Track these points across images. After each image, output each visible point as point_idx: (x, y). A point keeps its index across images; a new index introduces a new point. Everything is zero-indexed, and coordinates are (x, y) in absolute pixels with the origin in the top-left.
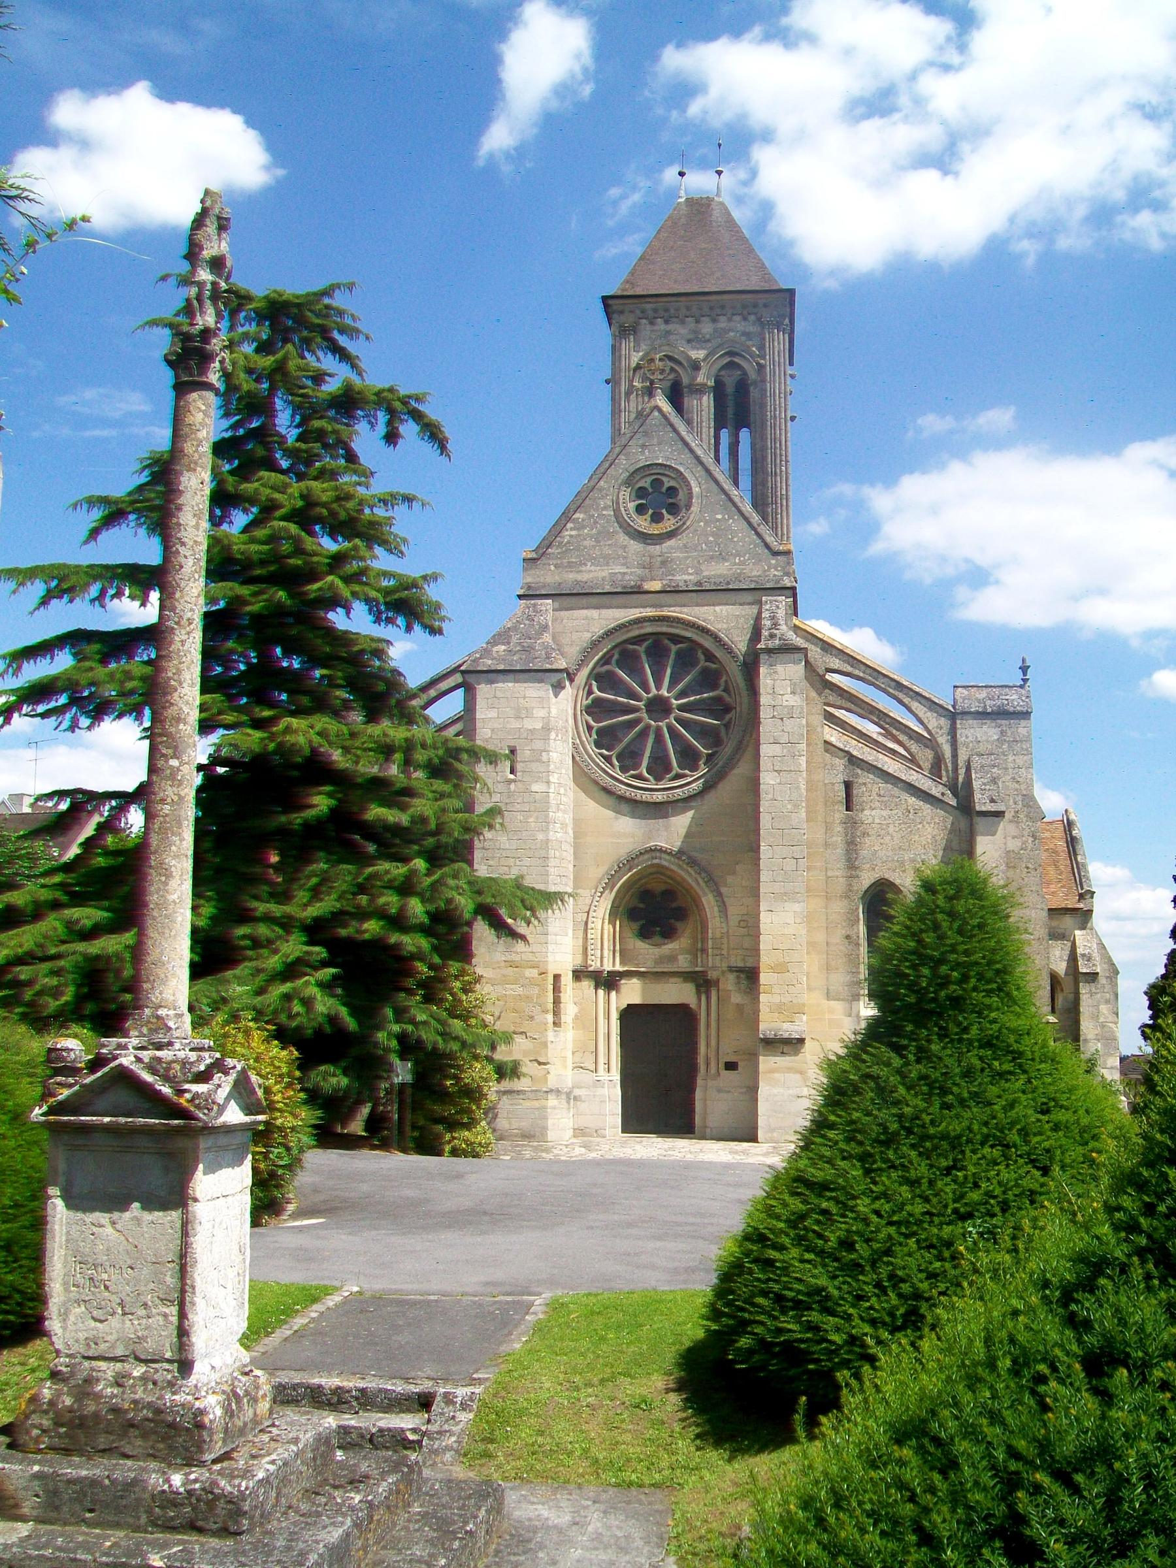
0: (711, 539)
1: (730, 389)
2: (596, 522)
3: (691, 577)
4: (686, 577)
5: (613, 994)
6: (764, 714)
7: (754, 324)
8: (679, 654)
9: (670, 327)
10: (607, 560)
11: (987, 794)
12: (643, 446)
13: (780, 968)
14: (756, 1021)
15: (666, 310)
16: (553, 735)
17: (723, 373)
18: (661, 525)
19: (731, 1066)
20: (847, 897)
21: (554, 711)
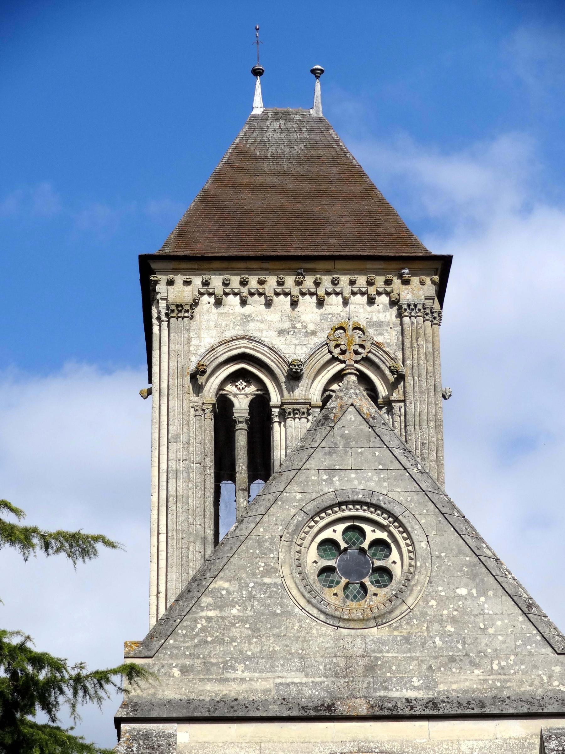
0: (450, 628)
2: (251, 597)
3: (420, 694)
4: (411, 694)
12: (331, 470)
15: (244, 283)
18: (364, 604)
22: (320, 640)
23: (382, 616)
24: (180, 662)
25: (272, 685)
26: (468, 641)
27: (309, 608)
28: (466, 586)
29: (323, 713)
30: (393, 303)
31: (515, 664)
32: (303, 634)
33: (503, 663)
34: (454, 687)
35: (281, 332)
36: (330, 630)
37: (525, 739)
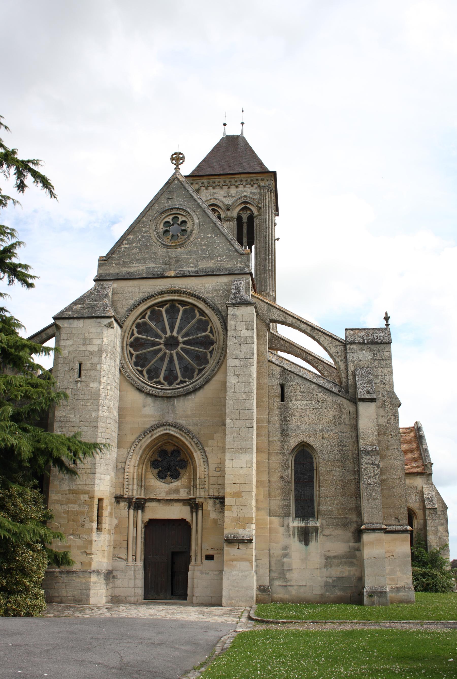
0: (204, 247)
1: (245, 220)
2: (140, 240)
3: (193, 269)
4: (190, 269)
5: (140, 512)
6: (230, 342)
7: (256, 188)
8: (185, 312)
9: (215, 191)
10: (145, 260)
11: (365, 389)
12: (168, 199)
13: (238, 495)
14: (223, 529)
15: (214, 182)
16: (104, 355)
17: (241, 212)
19: (210, 558)
20: (282, 453)
21: (106, 341)
22: (161, 253)
23: (182, 244)
24: (116, 262)
25: (145, 268)
26: (210, 251)
27: (158, 243)
28: (210, 234)
29: (160, 276)
30: (259, 186)
31: (225, 258)
32: (155, 251)
33: (222, 258)
34: (204, 266)
35: (224, 197)
36: (165, 250)
37: (227, 282)
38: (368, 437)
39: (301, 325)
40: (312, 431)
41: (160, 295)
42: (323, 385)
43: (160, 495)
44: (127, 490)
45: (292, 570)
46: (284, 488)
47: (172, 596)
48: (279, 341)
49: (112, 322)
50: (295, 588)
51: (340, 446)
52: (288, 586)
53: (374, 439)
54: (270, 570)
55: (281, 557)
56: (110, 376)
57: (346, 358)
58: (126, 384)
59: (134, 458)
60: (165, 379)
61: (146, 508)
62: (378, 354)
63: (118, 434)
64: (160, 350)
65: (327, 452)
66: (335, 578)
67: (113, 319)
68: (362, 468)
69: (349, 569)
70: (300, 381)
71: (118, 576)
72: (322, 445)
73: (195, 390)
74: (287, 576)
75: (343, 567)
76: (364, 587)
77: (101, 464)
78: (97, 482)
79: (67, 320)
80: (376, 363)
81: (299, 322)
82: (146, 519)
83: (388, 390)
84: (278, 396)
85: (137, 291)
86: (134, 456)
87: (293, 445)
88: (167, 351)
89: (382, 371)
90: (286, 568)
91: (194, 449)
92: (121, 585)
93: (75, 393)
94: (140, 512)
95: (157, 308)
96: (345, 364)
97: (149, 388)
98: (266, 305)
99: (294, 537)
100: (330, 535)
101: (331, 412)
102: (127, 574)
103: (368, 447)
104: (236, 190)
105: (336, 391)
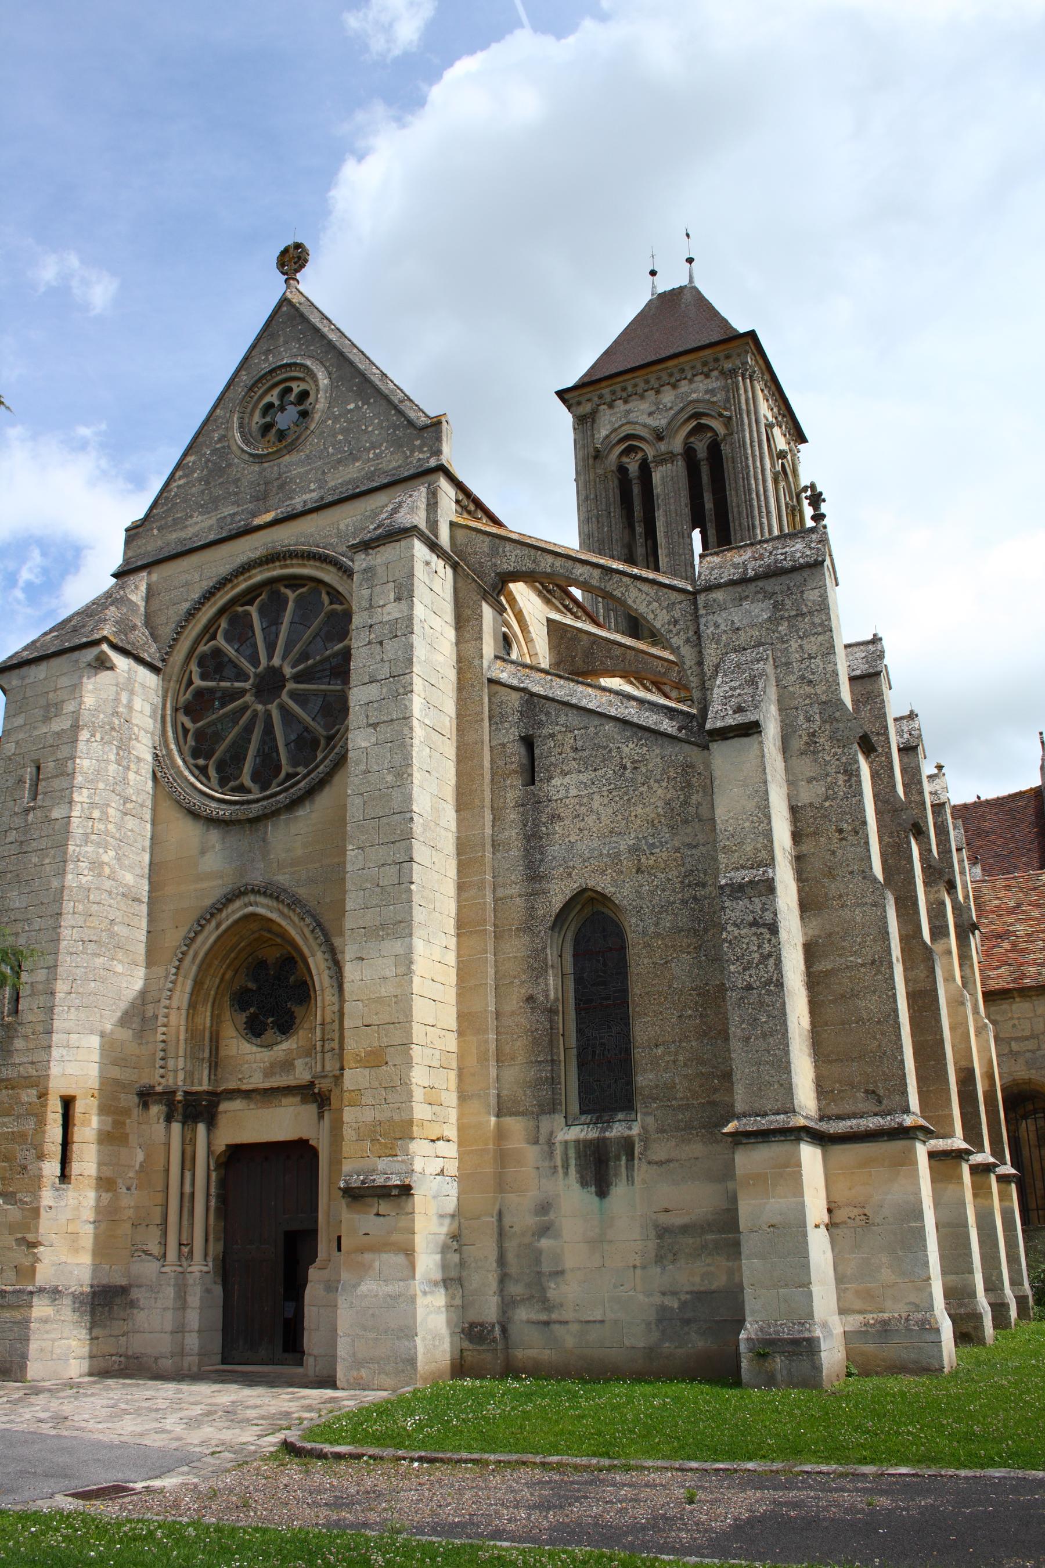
0: (340, 437)
1: (702, 452)
7: (717, 379)
8: (299, 600)
9: (628, 407)
11: (734, 702)
15: (624, 389)
16: (84, 735)
17: (692, 439)
24: (158, 524)
28: (355, 401)
31: (386, 449)
34: (340, 481)
35: (650, 414)
36: (256, 468)
38: (741, 844)
39: (574, 571)
40: (609, 855)
41: (242, 573)
42: (635, 720)
43: (252, 1080)
44: (162, 1071)
45: (562, 1273)
46: (537, 1030)
47: (286, 1355)
48: (609, 651)
49: (103, 652)
50: (574, 1327)
51: (689, 886)
52: (555, 1322)
53: (759, 846)
54: (503, 1279)
55: (533, 1235)
56: (101, 785)
57: (697, 633)
58: (166, 806)
59: (179, 988)
60: (255, 778)
61: (220, 1116)
62: (787, 601)
63: (149, 932)
64: (245, 708)
65: (652, 911)
66: (688, 1296)
67: (105, 647)
68: (725, 940)
69: (730, 1264)
70: (573, 719)
71: (142, 1302)
72: (637, 892)
73: (311, 793)
74: (551, 1294)
75: (709, 1260)
76: (740, 1323)
77: (69, 1007)
78: (55, 1053)
79: (17, 671)
80: (783, 628)
81: (570, 563)
82: (220, 1146)
83: (824, 698)
84: (516, 772)
85: (197, 577)
86: (179, 984)
87: (558, 902)
88: (260, 707)
89: (801, 646)
90: (546, 1268)
91: (309, 947)
92: (146, 1325)
93: (23, 839)
94: (201, 1128)
95: (240, 609)
96: (697, 649)
97: (214, 805)
98: (487, 539)
99: (566, 1174)
100: (669, 1161)
101: (660, 791)
102: (161, 1295)
103: (744, 872)
104: (675, 392)
105: (670, 730)
